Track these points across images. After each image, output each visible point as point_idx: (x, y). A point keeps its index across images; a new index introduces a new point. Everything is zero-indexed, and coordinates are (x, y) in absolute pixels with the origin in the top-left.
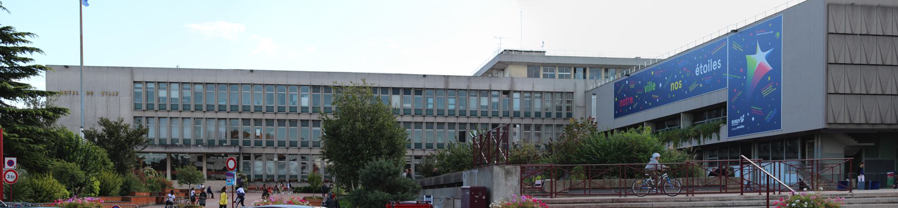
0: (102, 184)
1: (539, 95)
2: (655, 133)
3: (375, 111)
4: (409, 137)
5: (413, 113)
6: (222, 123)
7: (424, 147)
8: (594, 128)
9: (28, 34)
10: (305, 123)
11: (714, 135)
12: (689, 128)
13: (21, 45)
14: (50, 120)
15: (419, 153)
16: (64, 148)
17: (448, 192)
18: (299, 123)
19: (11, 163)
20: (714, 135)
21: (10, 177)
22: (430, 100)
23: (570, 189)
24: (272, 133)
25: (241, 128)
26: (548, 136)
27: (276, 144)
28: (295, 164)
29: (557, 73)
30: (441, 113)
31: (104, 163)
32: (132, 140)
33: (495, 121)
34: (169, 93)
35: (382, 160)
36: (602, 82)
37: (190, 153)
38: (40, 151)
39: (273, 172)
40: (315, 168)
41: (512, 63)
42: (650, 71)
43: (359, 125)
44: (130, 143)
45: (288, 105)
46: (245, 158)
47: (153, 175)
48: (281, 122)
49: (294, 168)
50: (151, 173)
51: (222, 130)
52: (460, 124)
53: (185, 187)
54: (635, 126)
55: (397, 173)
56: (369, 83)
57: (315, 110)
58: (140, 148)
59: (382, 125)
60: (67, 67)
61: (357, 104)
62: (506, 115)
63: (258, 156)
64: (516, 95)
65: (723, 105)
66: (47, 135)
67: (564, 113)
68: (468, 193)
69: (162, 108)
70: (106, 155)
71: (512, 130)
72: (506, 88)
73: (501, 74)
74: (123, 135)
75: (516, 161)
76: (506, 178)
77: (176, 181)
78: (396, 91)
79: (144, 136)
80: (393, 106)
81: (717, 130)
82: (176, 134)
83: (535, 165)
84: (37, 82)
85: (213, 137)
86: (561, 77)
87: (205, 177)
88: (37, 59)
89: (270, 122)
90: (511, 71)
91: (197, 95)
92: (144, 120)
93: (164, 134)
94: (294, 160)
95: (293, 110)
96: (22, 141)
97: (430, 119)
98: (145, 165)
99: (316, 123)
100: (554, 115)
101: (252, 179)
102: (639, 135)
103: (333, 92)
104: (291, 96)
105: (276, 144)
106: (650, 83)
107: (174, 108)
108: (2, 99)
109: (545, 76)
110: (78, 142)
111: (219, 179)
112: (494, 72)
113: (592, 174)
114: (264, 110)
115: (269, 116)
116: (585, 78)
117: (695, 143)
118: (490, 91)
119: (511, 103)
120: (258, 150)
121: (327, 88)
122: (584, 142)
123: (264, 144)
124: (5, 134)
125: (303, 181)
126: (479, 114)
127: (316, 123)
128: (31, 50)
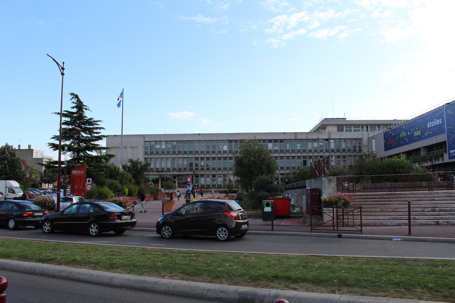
0: (129, 190)
1: (344, 140)
2: (407, 158)
3: (260, 152)
4: (278, 164)
5: (279, 152)
6: (185, 160)
7: (285, 169)
8: (374, 157)
9: (99, 121)
10: (225, 158)
11: (440, 159)
12: (426, 155)
13: (96, 126)
14: (107, 160)
15: (282, 172)
16: (113, 173)
17: (298, 191)
18: (222, 159)
19: (89, 181)
20: (440, 159)
21: (89, 188)
22: (288, 145)
23: (363, 189)
24: (209, 164)
25: (194, 162)
26: (350, 161)
27: (211, 169)
28: (221, 179)
29: (353, 129)
30: (293, 151)
31: (130, 181)
32: (143, 169)
33: (322, 154)
34: (161, 146)
35: (264, 176)
36: (376, 132)
37: (170, 175)
38: (102, 175)
39: (209, 183)
40: (230, 181)
41: (329, 125)
42: (402, 126)
43: (252, 158)
44: (142, 170)
45: (217, 150)
46: (196, 176)
47: (152, 185)
48: (214, 158)
49: (220, 180)
50: (152, 185)
51: (185, 163)
52: (298, 156)
53: (167, 191)
54: (397, 155)
55: (272, 182)
56: (258, 138)
57: (230, 152)
58: (146, 173)
59: (264, 158)
60: (115, 136)
61: (251, 148)
62: (327, 151)
63: (202, 176)
64: (332, 141)
65: (444, 143)
66: (106, 167)
67: (357, 149)
68: (309, 192)
69: (157, 153)
70: (131, 176)
71: (331, 158)
72: (326, 137)
73: (323, 131)
74: (139, 166)
75: (333, 174)
76: (329, 183)
77: (163, 189)
78: (270, 141)
79: (149, 167)
80: (269, 148)
81: (442, 156)
82: (163, 166)
83: (343, 176)
84: (102, 143)
85: (181, 167)
86: (355, 131)
87: (177, 186)
88: (103, 133)
89: (208, 159)
90: (329, 129)
91: (174, 147)
92: (149, 159)
93: (158, 166)
94: (220, 177)
95: (219, 152)
96: (94, 171)
97: (288, 155)
98: (149, 181)
99: (231, 158)
100: (352, 150)
101: (199, 187)
102: (399, 159)
103: (239, 142)
104: (218, 145)
105: (211, 169)
106: (403, 132)
107: (163, 153)
108: (87, 151)
109: (347, 131)
110: (119, 170)
111: (184, 187)
112: (320, 129)
113: (374, 180)
114: (205, 153)
115: (208, 156)
116: (367, 131)
117: (430, 163)
118: (318, 139)
119: (329, 145)
120: (202, 173)
121: (236, 141)
122: (370, 163)
123: (205, 169)
124: (87, 167)
125: (224, 187)
126: (313, 151)
127: (231, 158)
128: (100, 128)
